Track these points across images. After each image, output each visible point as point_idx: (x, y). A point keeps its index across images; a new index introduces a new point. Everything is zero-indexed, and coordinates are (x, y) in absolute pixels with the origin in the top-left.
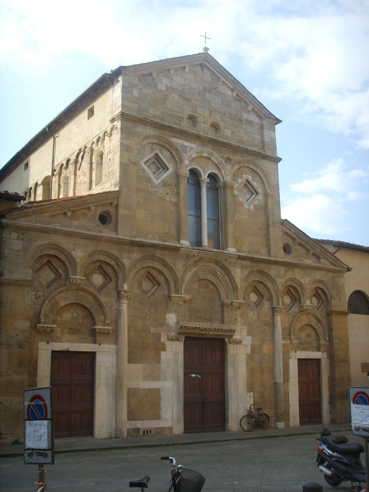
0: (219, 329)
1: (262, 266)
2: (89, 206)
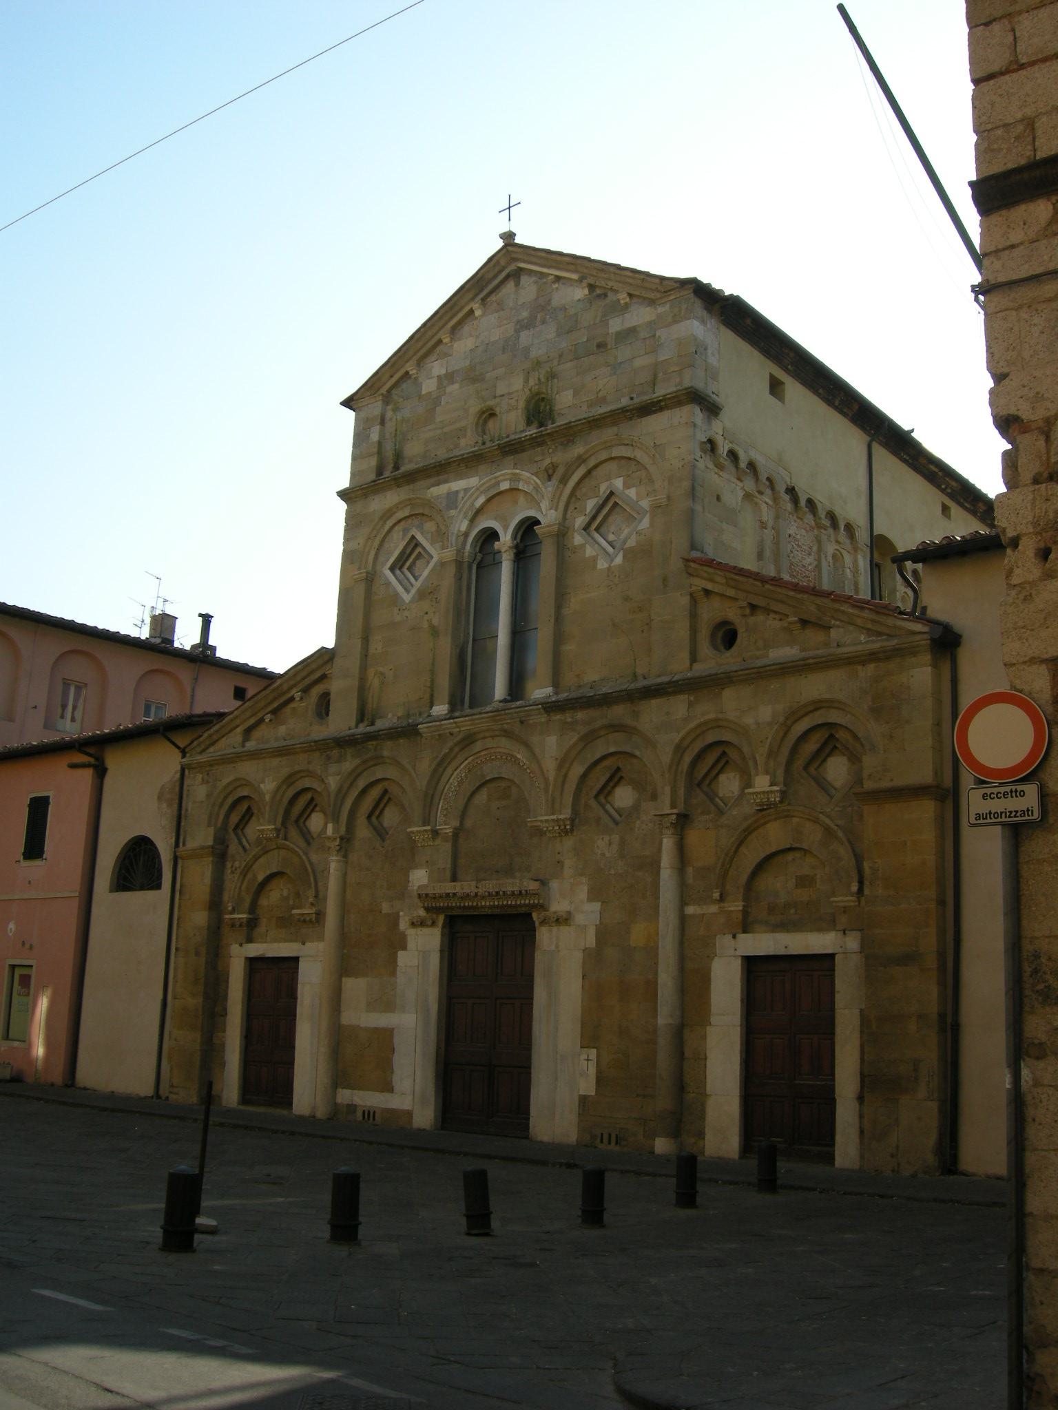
0: (497, 893)
1: (619, 712)
2: (289, 695)
